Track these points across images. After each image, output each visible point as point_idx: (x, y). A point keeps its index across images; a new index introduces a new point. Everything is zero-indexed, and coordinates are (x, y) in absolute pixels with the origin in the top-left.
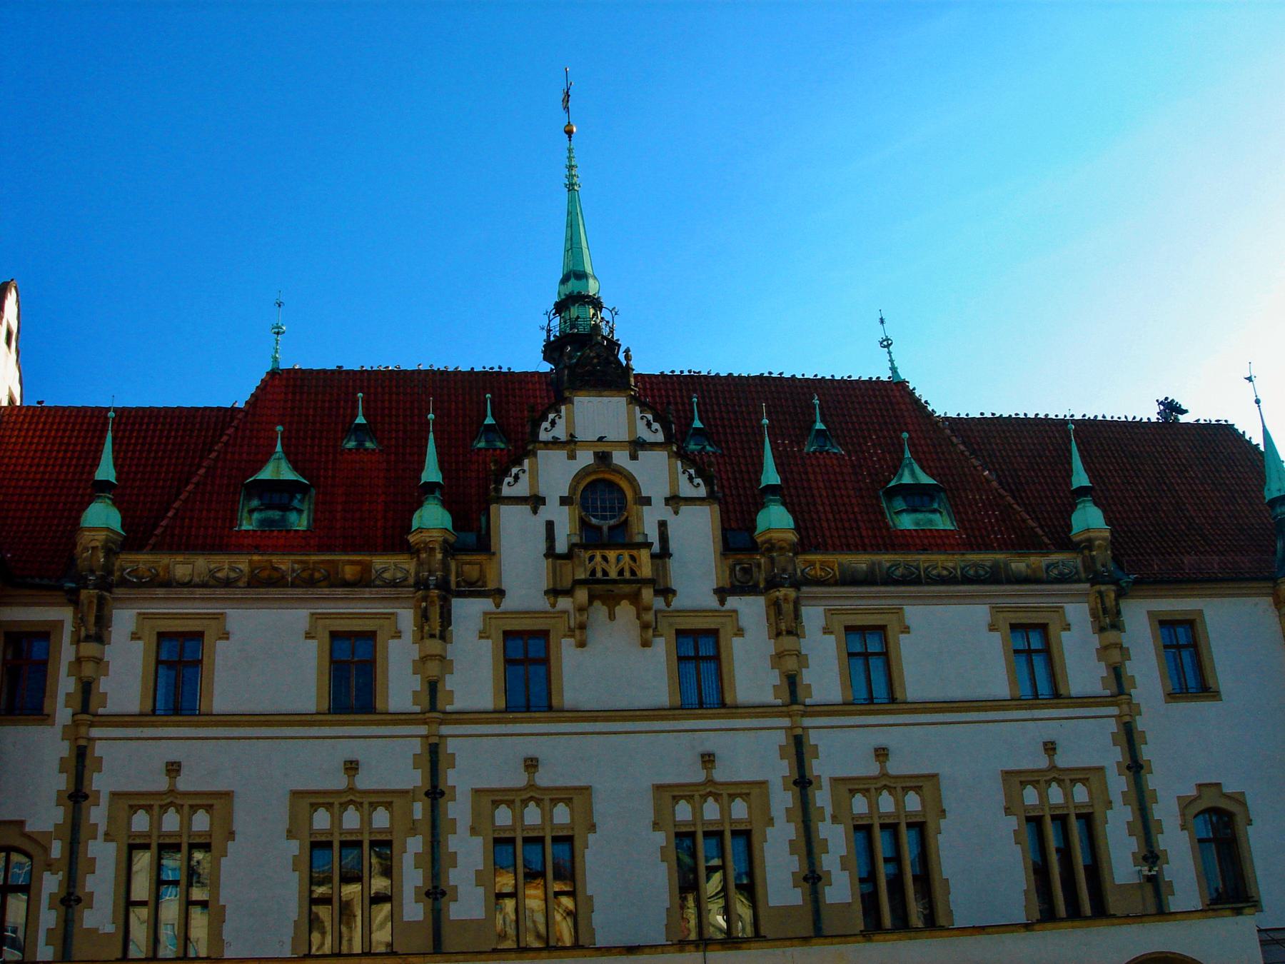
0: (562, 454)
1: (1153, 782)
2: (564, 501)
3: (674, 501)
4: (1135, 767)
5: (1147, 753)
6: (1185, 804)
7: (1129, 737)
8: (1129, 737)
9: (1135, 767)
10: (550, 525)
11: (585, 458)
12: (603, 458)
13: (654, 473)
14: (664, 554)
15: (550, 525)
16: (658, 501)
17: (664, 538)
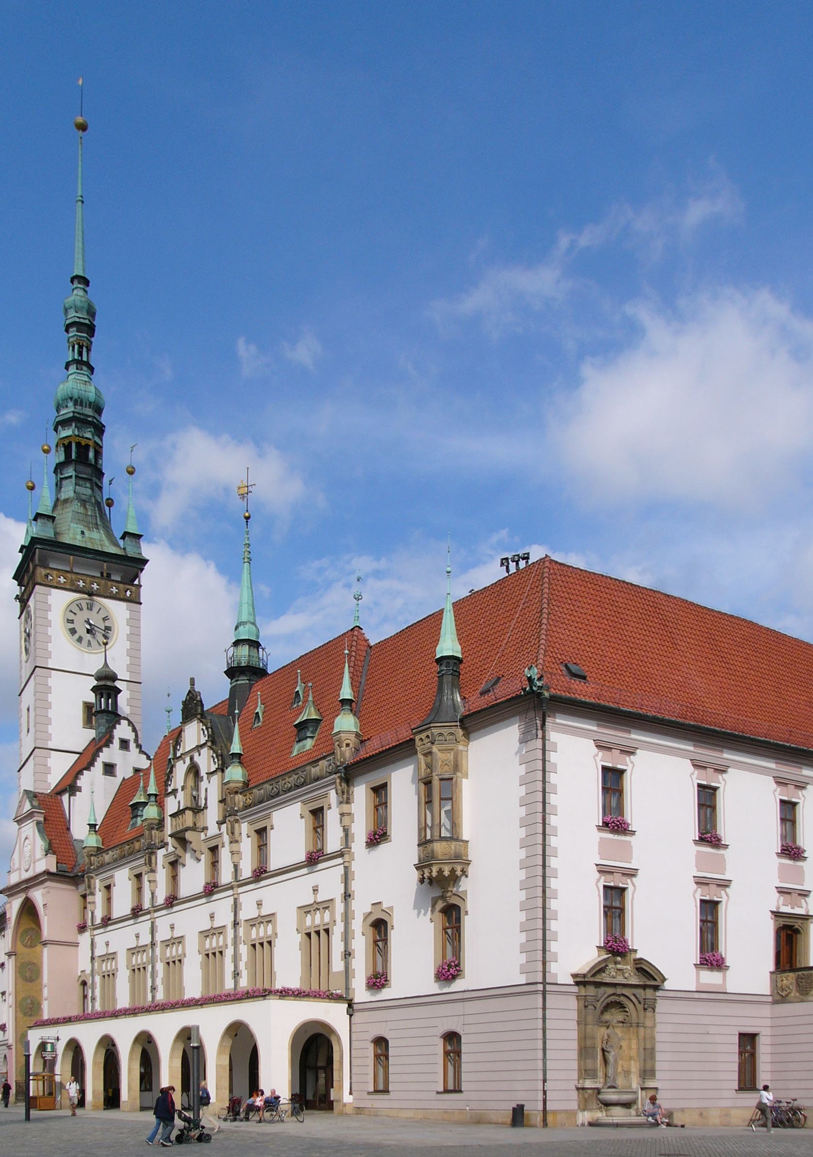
0: (182, 762)
1: (355, 904)
2: (183, 788)
3: (210, 774)
4: (347, 896)
5: (354, 886)
6: (367, 916)
7: (347, 878)
8: (347, 878)
9: (347, 896)
10: (179, 802)
11: (188, 760)
12: (192, 758)
13: (205, 761)
14: (206, 807)
15: (179, 802)
16: (205, 776)
17: (206, 799)
